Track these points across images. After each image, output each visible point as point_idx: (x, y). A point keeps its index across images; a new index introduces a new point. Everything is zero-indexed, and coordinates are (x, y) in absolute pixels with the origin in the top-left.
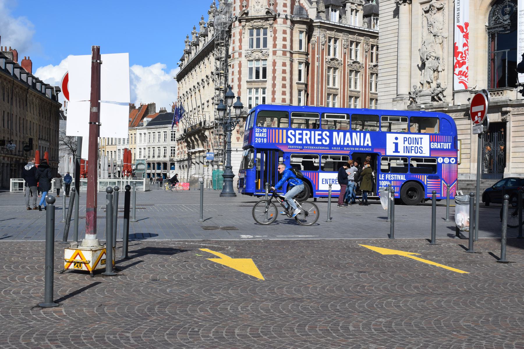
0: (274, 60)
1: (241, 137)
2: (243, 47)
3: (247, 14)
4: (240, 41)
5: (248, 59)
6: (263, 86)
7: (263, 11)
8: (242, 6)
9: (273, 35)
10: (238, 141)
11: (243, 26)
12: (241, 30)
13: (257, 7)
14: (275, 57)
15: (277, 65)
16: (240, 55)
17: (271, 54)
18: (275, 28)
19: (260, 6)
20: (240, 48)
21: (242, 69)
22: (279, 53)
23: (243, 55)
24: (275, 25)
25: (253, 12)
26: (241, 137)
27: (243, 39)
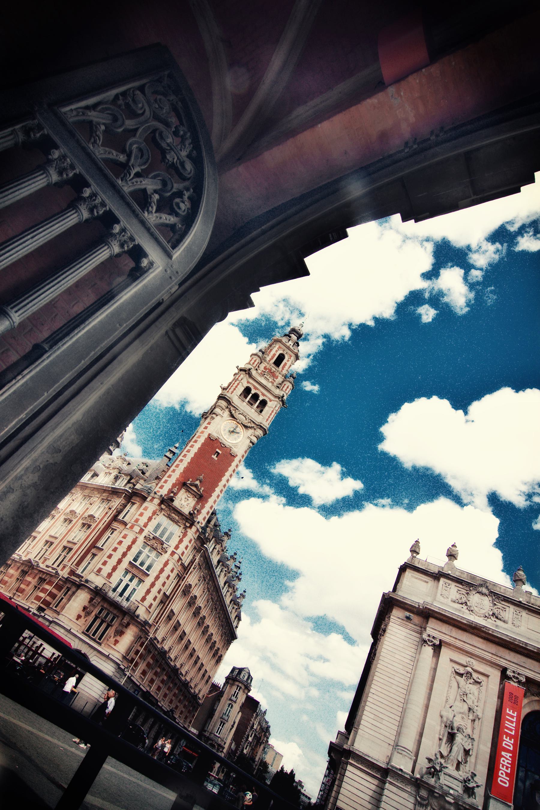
0: (168, 560)
1: (83, 617)
2: (148, 526)
3: (172, 501)
4: (150, 519)
5: (145, 541)
6: (142, 578)
7: (186, 509)
8: (171, 491)
9: (181, 537)
10: (77, 619)
11: (162, 509)
12: (157, 510)
13: (183, 502)
14: (170, 558)
15: (168, 566)
16: (141, 531)
17: (169, 552)
18: (187, 532)
19: (186, 503)
20: (145, 525)
21: (133, 546)
22: (176, 557)
23: (144, 534)
24: (188, 530)
25: (178, 503)
26: (83, 617)
27: (153, 519)
